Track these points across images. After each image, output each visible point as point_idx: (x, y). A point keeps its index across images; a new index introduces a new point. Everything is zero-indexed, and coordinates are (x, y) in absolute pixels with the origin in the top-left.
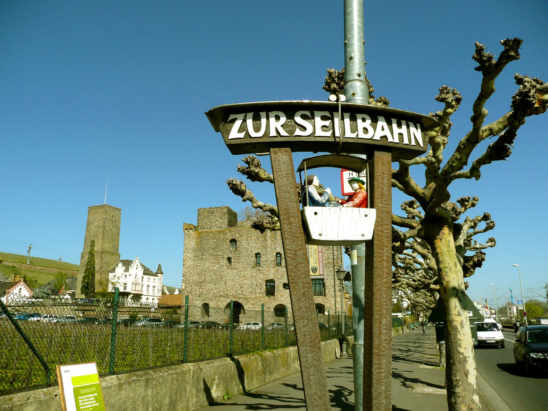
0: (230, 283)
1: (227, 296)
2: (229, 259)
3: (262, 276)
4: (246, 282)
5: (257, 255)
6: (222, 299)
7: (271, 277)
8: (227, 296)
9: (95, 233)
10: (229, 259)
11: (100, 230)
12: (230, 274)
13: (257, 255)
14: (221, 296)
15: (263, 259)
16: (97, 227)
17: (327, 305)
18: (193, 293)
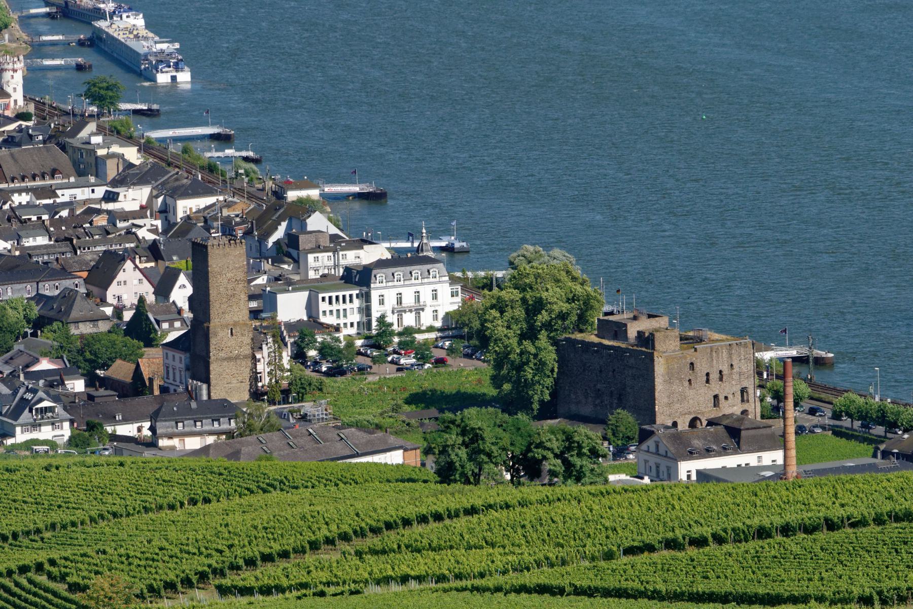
0: (691, 401)
1: (690, 413)
2: (690, 381)
3: (711, 392)
4: (701, 399)
5: (708, 374)
6: (687, 416)
7: (716, 393)
8: (690, 413)
9: (230, 292)
10: (690, 381)
11: (240, 286)
12: (690, 393)
13: (708, 374)
14: (686, 414)
15: (711, 376)
16: (234, 280)
17: (750, 410)
18: (665, 414)
